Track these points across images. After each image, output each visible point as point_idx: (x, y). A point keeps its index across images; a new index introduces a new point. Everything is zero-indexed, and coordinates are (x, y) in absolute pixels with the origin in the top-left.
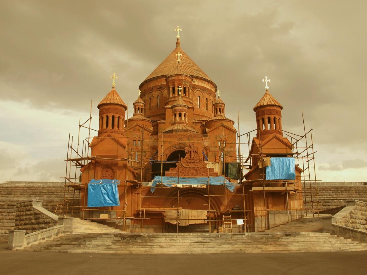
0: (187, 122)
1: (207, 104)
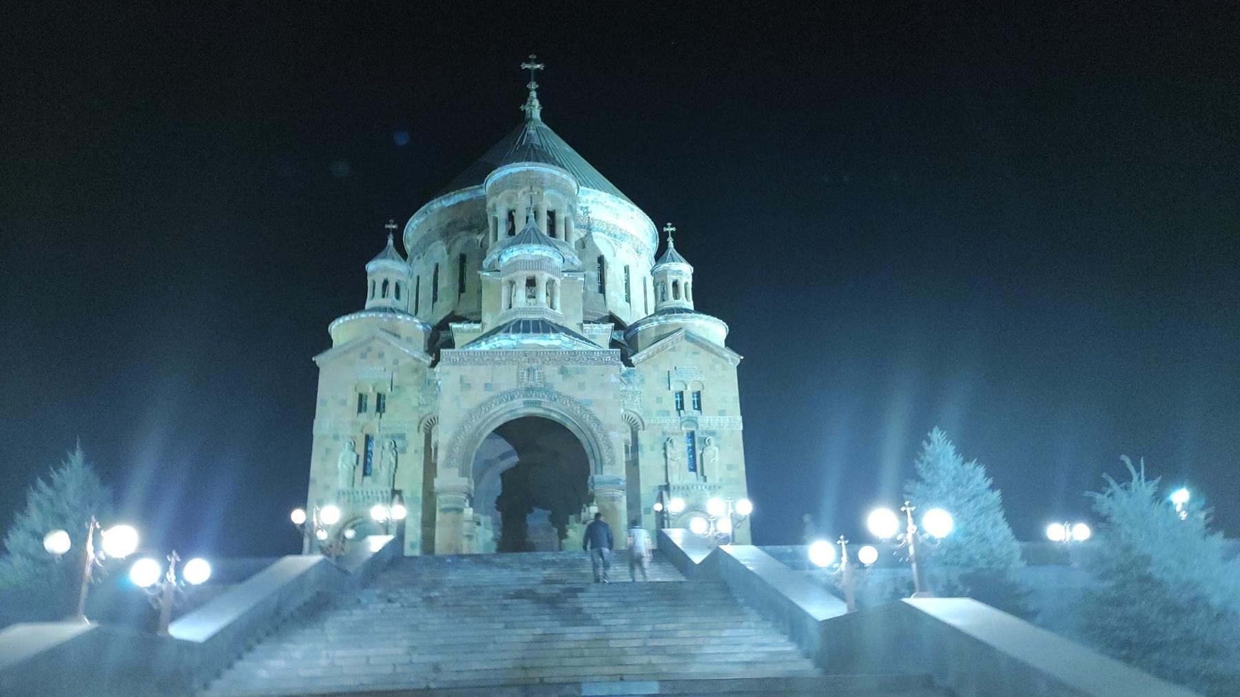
0: (560, 312)
1: (626, 284)
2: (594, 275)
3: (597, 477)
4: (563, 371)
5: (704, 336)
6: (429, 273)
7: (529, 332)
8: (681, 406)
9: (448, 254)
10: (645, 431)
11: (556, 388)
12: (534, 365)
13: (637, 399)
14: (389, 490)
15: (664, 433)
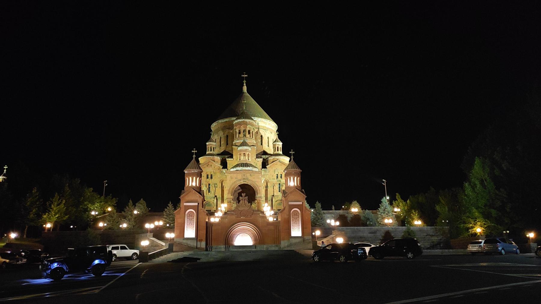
2: (260, 141)
3: (257, 196)
4: (250, 175)
5: (283, 161)
6: (219, 139)
7: (243, 166)
8: (277, 177)
9: (224, 135)
10: (269, 183)
11: (249, 179)
12: (245, 174)
13: (268, 175)
14: (214, 196)
15: (273, 184)
